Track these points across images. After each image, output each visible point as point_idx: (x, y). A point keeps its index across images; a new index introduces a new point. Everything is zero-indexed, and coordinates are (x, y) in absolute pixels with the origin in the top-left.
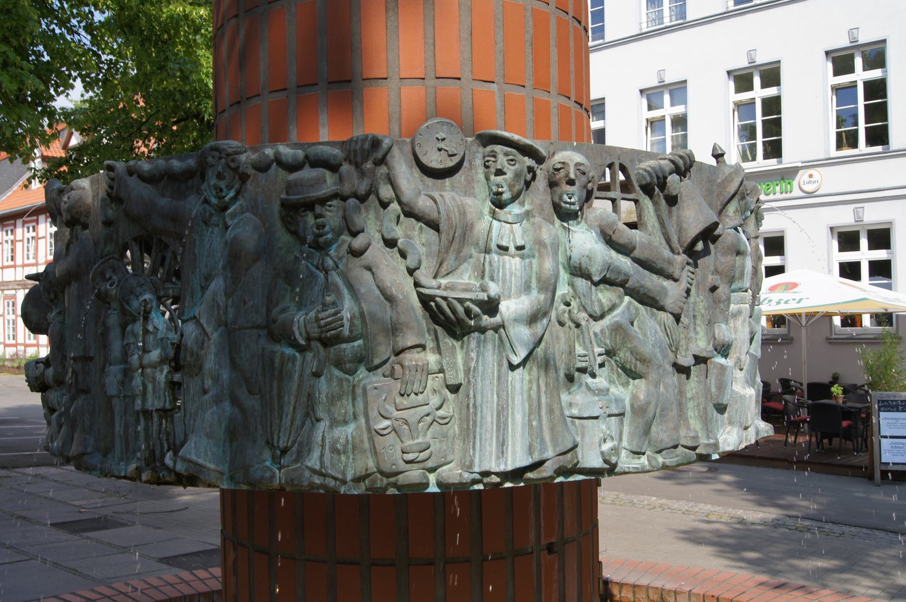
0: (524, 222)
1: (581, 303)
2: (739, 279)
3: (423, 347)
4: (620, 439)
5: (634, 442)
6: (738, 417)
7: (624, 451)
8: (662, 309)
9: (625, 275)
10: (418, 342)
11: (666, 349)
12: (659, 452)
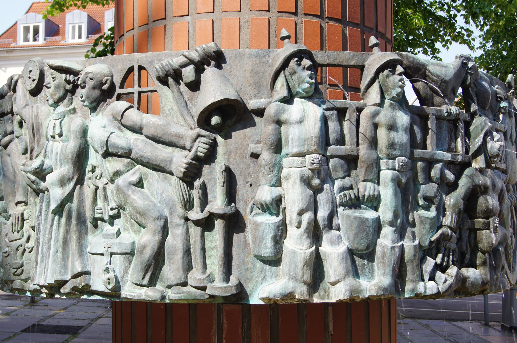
0: (66, 117)
1: (101, 171)
2: (286, 145)
3: (26, 203)
4: (126, 272)
5: (135, 276)
6: (287, 269)
7: (129, 282)
8: (172, 174)
9: (123, 149)
10: (24, 200)
11: (174, 205)
12: (169, 287)
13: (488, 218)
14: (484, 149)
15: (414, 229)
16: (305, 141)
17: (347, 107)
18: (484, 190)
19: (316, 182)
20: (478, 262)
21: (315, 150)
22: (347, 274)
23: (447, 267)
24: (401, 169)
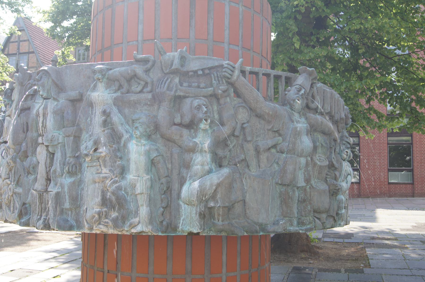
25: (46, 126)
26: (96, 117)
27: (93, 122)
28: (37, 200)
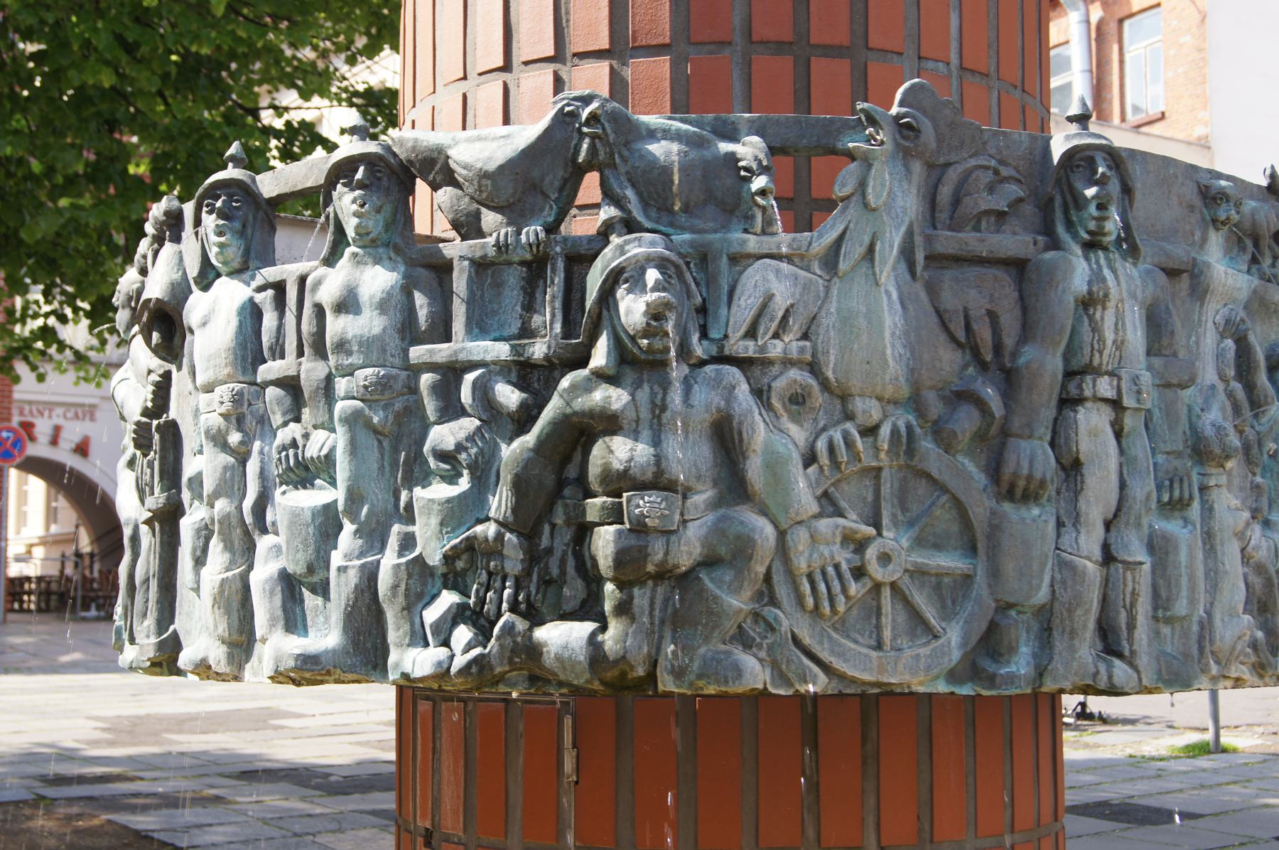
13: (620, 496)
14: (611, 319)
15: (410, 529)
16: (209, 361)
17: (284, 277)
18: (609, 423)
19: (235, 438)
20: (608, 607)
21: (229, 375)
22: (274, 625)
23: (499, 615)
24: (363, 395)
25: (1123, 342)
26: (1208, 335)
27: (1201, 349)
28: (1094, 592)
